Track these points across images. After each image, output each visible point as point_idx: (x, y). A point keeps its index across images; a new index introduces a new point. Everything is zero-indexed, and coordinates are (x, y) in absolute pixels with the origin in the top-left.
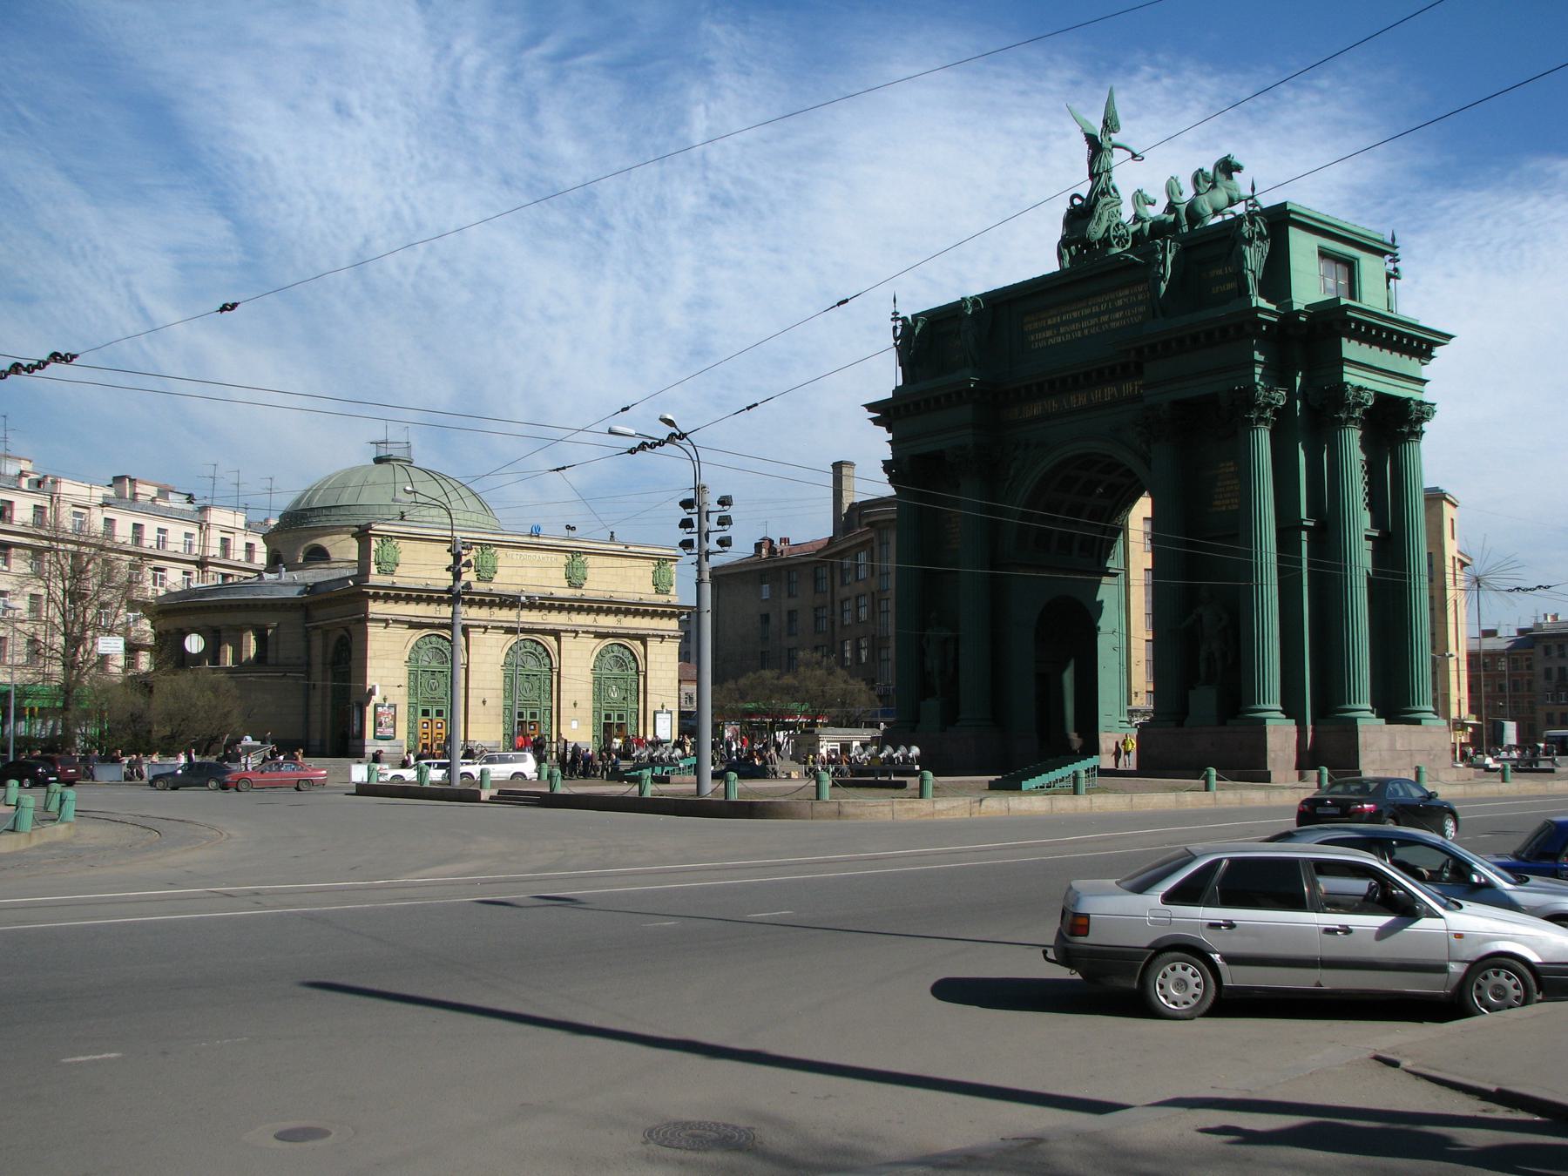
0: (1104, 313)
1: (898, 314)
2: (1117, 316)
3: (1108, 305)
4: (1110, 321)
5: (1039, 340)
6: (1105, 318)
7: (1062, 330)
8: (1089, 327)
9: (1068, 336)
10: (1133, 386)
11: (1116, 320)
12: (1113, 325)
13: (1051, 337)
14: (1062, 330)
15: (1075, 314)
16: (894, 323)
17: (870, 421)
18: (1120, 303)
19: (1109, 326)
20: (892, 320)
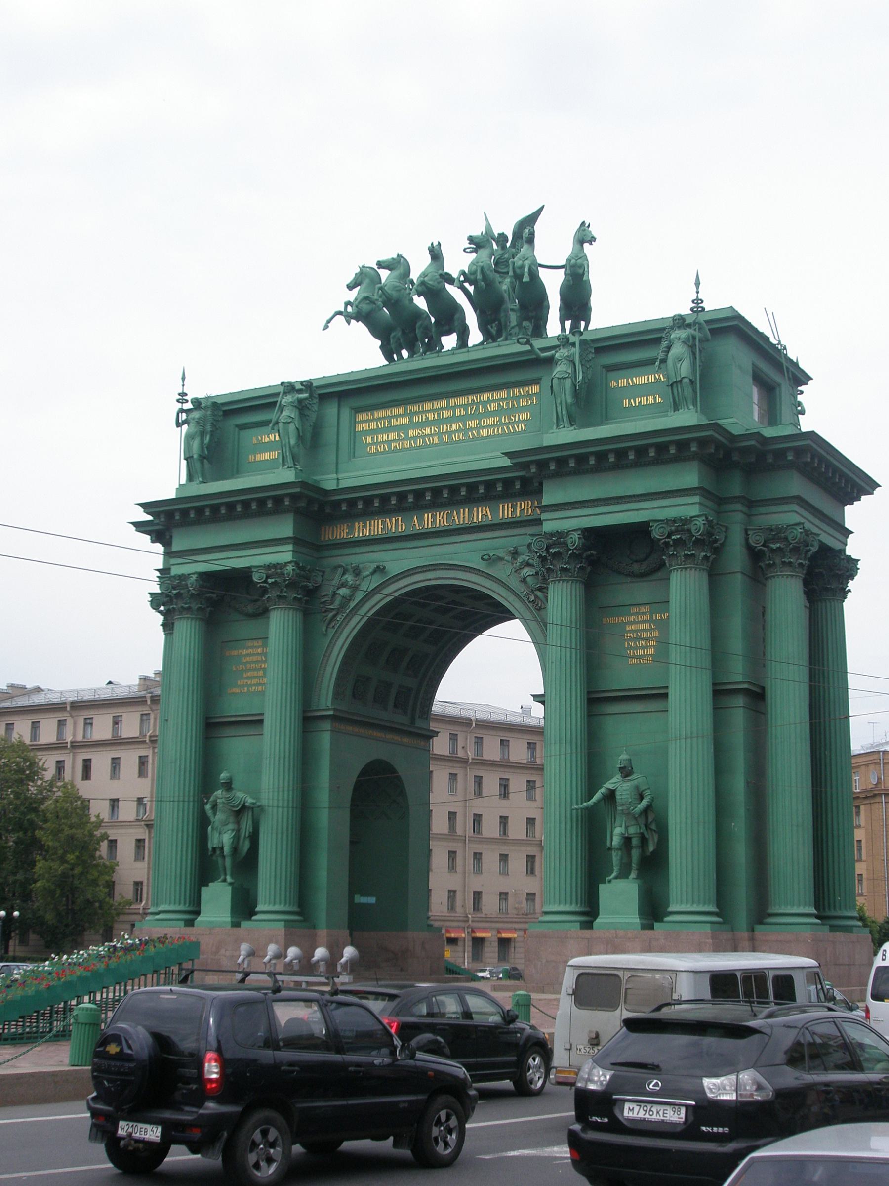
0: (472, 417)
1: (186, 395)
2: (490, 421)
3: (477, 408)
4: (479, 427)
5: (378, 443)
6: (473, 424)
7: (411, 433)
8: (450, 433)
9: (420, 442)
10: (514, 507)
11: (489, 426)
12: (483, 433)
13: (394, 440)
14: (411, 433)
15: (431, 416)
16: (179, 406)
17: (131, 526)
18: (494, 406)
19: (478, 433)
20: (178, 401)
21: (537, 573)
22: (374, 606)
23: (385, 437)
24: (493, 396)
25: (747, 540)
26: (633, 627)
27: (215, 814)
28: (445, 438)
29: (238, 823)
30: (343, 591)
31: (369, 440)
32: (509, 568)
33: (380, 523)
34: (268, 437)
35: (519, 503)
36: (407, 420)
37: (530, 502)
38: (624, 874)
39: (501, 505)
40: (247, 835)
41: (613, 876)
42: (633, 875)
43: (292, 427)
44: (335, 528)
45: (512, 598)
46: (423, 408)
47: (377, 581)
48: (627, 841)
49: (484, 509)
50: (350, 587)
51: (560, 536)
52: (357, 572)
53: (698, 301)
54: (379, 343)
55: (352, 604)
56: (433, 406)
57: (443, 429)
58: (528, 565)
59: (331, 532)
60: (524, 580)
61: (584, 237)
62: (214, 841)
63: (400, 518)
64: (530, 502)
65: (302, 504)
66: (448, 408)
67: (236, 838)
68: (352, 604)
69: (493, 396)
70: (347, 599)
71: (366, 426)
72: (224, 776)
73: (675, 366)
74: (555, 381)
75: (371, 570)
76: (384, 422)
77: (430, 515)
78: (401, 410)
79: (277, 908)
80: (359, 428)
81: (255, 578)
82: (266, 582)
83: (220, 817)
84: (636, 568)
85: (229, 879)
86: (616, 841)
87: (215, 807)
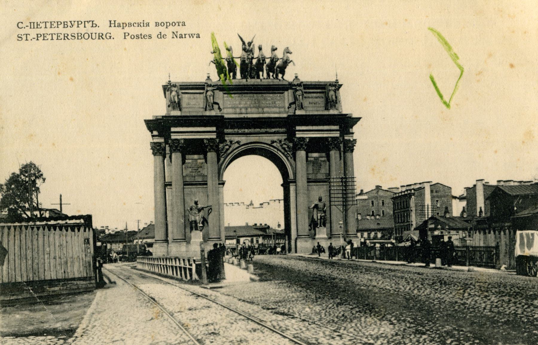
30: (227, 147)
32: (278, 145)
38: (321, 226)
41: (318, 226)
47: (237, 145)
48: (321, 217)
51: (304, 139)
52: (231, 142)
53: (337, 80)
55: (229, 151)
60: (284, 149)
61: (287, 51)
68: (229, 151)
86: (319, 217)
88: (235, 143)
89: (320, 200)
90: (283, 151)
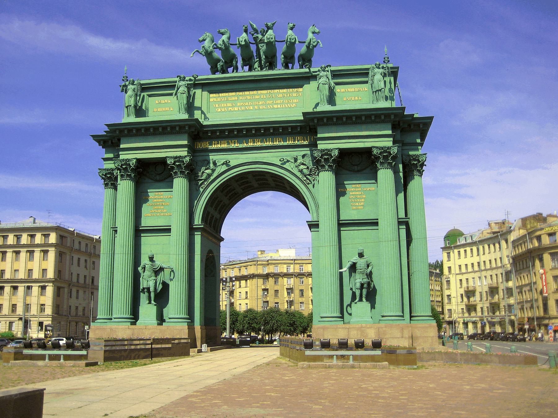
9: (243, 108)
12: (275, 106)
15: (249, 97)
17: (91, 137)
18: (281, 95)
19: (273, 106)
21: (308, 168)
22: (221, 181)
23: (225, 105)
24: (280, 91)
25: (402, 159)
26: (353, 193)
27: (144, 272)
28: (256, 107)
29: (156, 277)
30: (208, 171)
31: (217, 106)
32: (293, 165)
33: (226, 142)
34: (164, 101)
35: (296, 137)
36: (236, 98)
37: (302, 137)
38: (361, 300)
39: (288, 138)
40: (161, 282)
41: (357, 300)
42: (364, 299)
43: (185, 96)
44: (202, 143)
45: (294, 178)
46: (244, 94)
47: (224, 168)
48: (362, 285)
49: (279, 139)
50: (212, 170)
54: (210, 67)
55: (212, 178)
56: (250, 93)
57: (255, 103)
58: (303, 164)
59: (200, 144)
60: (301, 171)
62: (143, 284)
63: (236, 141)
64: (302, 137)
65: (193, 130)
66: (258, 95)
67: (156, 283)
68: (212, 178)
69: (280, 91)
70: (209, 176)
71: (215, 100)
72: (150, 254)
73: (378, 83)
74: (321, 85)
75: (222, 162)
76: (225, 98)
77: (252, 140)
78: (233, 94)
79: (125, 316)
80: (211, 100)
81: (169, 162)
82: (174, 164)
83: (147, 273)
84: (356, 168)
85: (153, 302)
86: (358, 285)
87: (144, 268)
88: (223, 164)
89: (361, 255)
90: (299, 174)
